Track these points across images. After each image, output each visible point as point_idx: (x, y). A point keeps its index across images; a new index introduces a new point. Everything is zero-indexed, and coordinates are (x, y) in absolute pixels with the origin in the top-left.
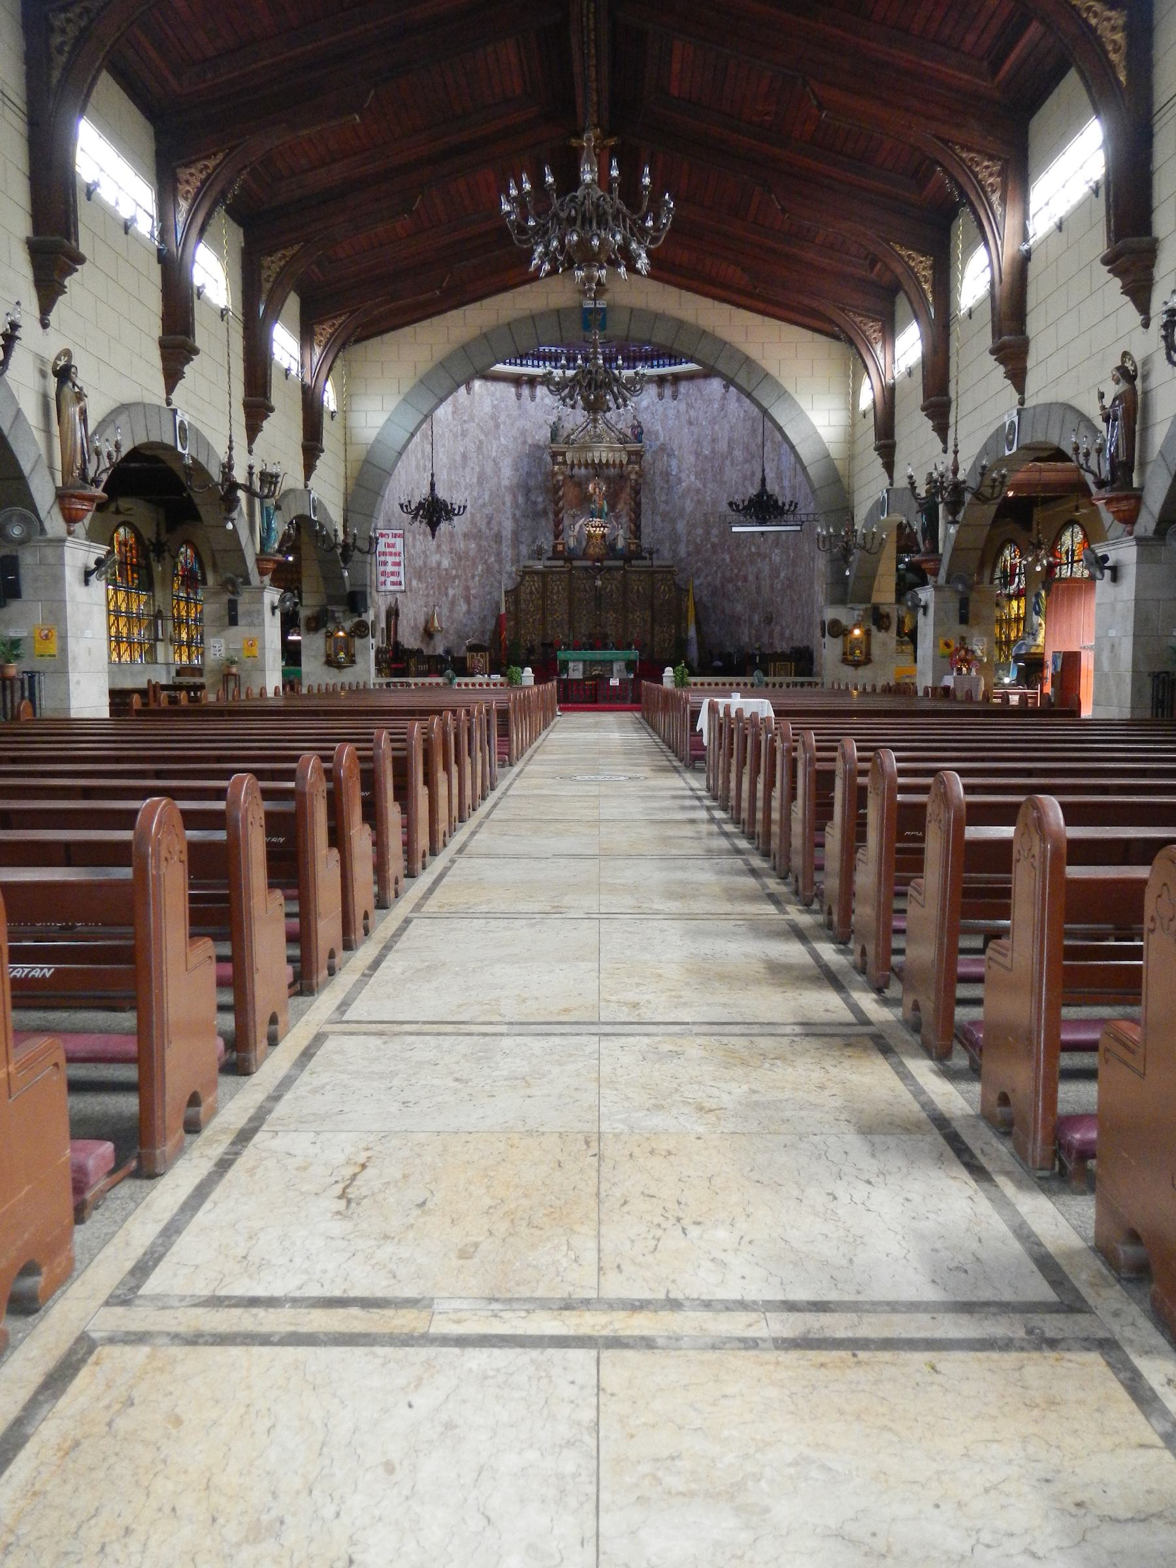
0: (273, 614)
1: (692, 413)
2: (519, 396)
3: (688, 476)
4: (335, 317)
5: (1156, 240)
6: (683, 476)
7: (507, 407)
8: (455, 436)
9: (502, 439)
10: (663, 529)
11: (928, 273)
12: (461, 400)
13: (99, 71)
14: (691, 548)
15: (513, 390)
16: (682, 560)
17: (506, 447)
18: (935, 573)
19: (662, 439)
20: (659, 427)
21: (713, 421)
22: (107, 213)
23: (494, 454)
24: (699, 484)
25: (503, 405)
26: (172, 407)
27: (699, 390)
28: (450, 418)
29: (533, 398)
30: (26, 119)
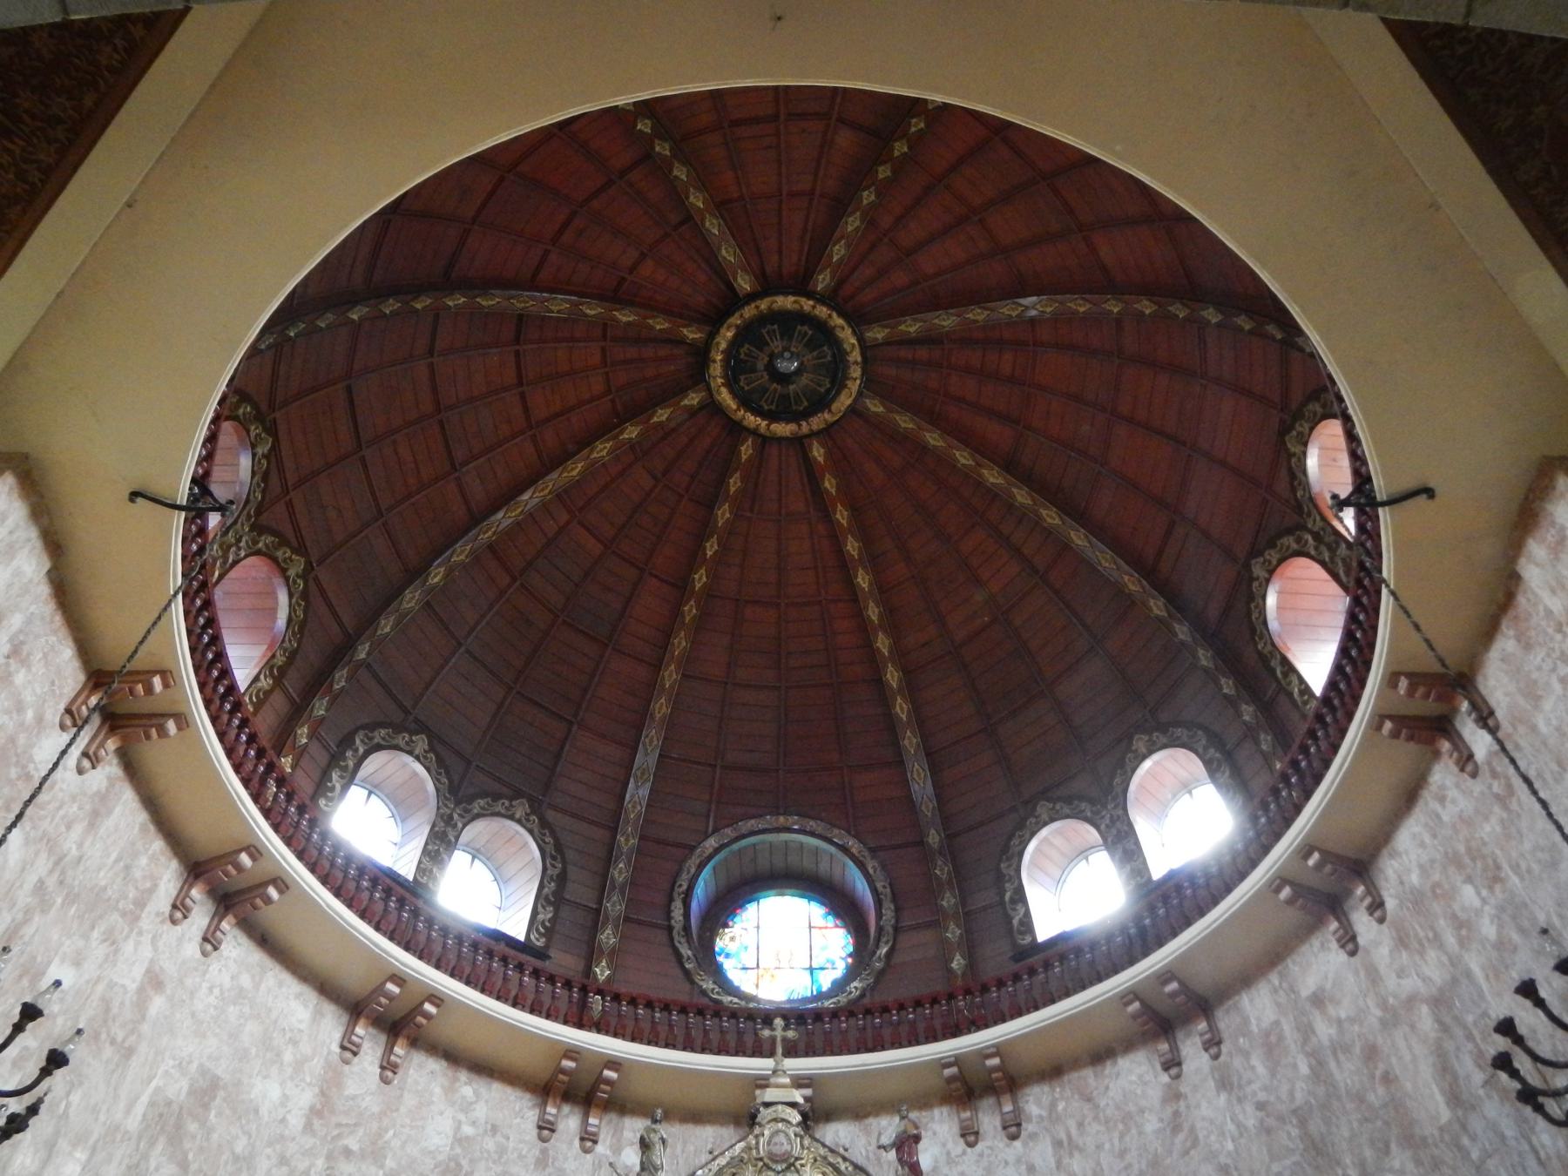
2: (546, 1128)
7: (502, 1151)
12: (351, 1088)
15: (532, 1116)
25: (490, 1144)
27: (1089, 1100)
28: (296, 1121)
29: (588, 1139)
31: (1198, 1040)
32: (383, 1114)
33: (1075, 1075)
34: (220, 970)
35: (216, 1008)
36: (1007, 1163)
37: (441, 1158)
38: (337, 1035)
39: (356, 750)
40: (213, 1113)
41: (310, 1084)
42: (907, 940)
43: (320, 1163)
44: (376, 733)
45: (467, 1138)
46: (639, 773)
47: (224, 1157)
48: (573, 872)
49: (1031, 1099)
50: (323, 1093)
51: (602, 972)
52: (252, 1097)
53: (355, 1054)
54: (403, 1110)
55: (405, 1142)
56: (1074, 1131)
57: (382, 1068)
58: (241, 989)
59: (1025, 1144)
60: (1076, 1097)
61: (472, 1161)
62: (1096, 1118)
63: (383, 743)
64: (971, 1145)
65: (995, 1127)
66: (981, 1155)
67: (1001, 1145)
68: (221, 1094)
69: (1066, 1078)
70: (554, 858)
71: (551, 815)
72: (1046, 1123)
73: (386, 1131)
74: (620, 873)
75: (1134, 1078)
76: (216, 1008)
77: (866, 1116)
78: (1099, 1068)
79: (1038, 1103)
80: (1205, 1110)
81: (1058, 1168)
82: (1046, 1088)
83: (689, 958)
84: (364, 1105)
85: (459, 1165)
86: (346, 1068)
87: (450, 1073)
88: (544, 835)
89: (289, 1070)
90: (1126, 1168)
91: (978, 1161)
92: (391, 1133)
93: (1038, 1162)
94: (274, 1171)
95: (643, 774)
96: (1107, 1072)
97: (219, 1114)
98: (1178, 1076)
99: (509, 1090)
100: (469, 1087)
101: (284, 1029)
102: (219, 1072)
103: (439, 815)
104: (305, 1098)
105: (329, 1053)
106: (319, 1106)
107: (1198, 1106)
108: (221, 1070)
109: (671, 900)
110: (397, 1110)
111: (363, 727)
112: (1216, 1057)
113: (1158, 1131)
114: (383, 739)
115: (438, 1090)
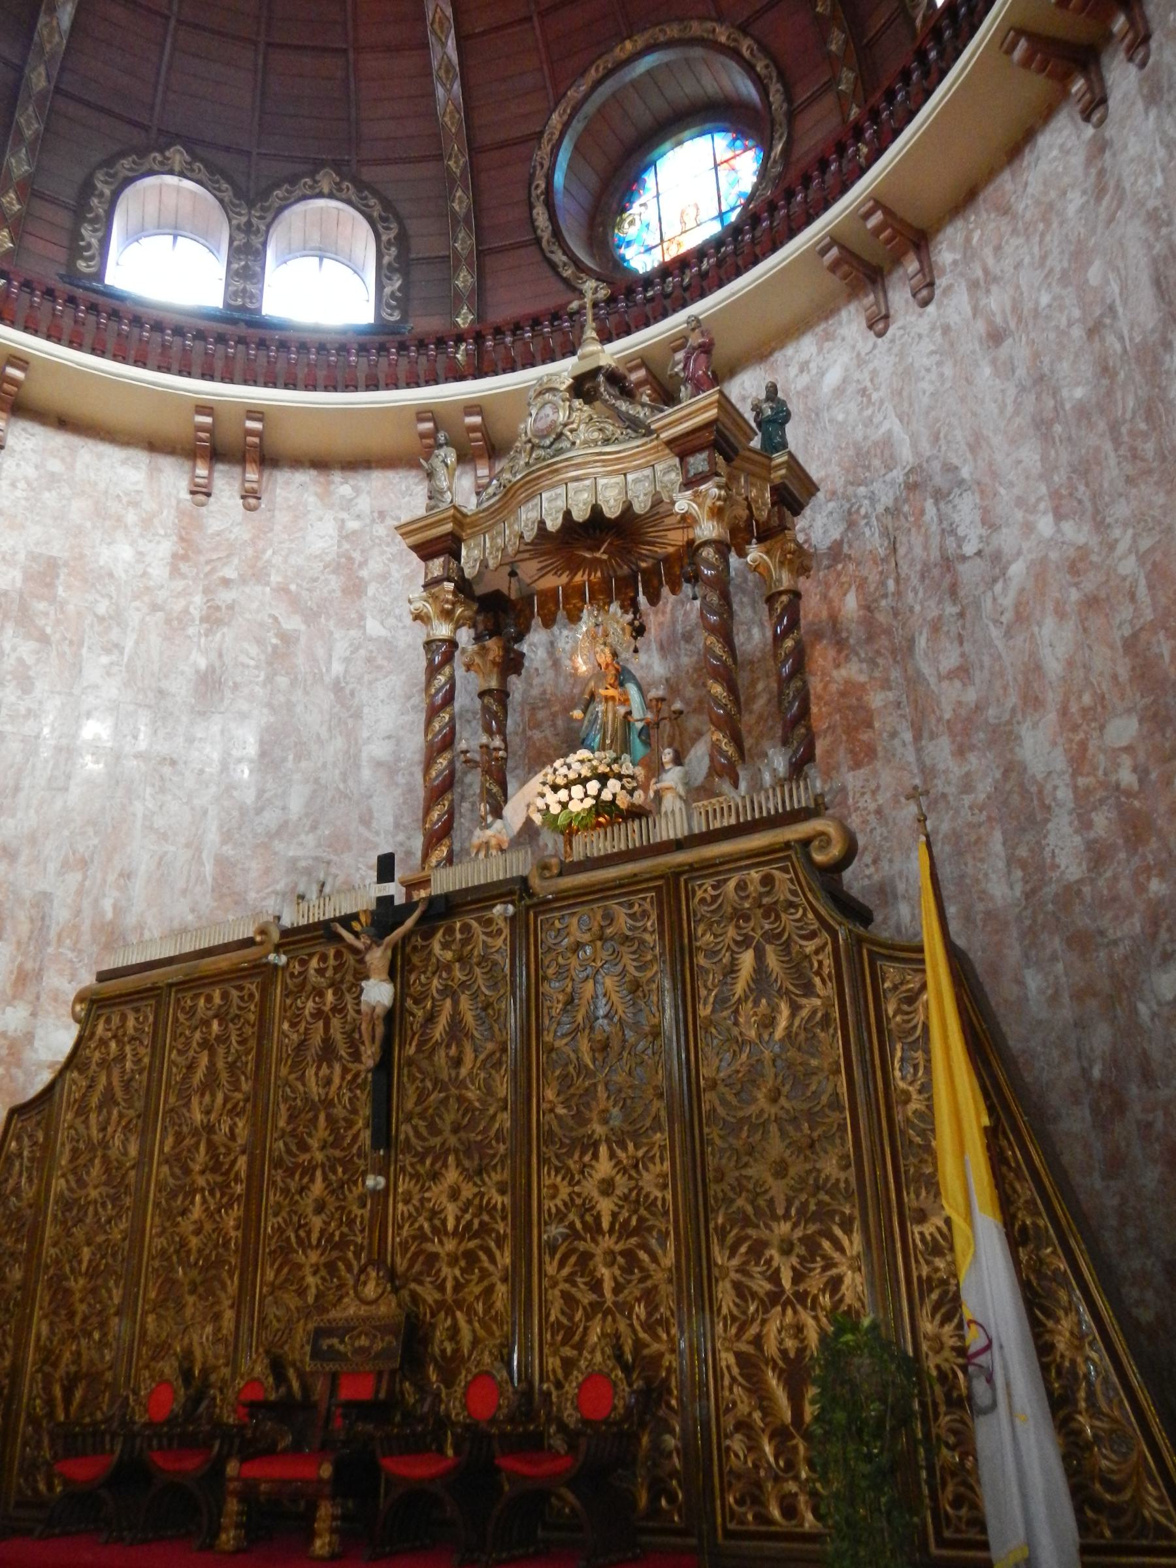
1: (996, 301)
3: (1028, 528)
6: (1008, 539)
8: (175, 624)
9: (373, 627)
10: (967, 786)
14: (1102, 821)
16: (1071, 892)
17: (388, 646)
19: (906, 454)
20: (891, 424)
21: (1080, 255)
23: (337, 668)
24: (1076, 533)
28: (159, 571)
31: (1121, 55)
32: (253, 541)
33: (991, 188)
34: (18, 465)
35: (27, 499)
36: (920, 336)
37: (328, 559)
38: (183, 485)
39: (102, 195)
40: (60, 591)
41: (166, 535)
42: (806, 121)
43: (198, 599)
44: (118, 166)
45: (354, 533)
46: (442, 73)
47: (88, 622)
48: (413, 226)
49: (944, 246)
50: (182, 539)
51: (464, 319)
52: (102, 563)
53: (208, 495)
54: (278, 528)
55: (287, 556)
56: (990, 261)
57: (243, 497)
58: (53, 474)
59: (939, 307)
60: (993, 216)
61: (363, 551)
62: (1015, 232)
63: (130, 174)
64: (880, 335)
65: (907, 301)
66: (892, 341)
67: (913, 319)
68: (63, 572)
69: (981, 198)
70: (384, 220)
71: (368, 174)
72: (960, 268)
73: (264, 551)
74: (461, 202)
75: (1055, 153)
76: (27, 499)
77: (771, 353)
78: (1016, 163)
79: (952, 248)
80: (1134, 148)
81: (974, 315)
82: (959, 223)
83: (565, 264)
84: (233, 536)
85: (350, 559)
86: (203, 510)
87: (322, 479)
88: (366, 198)
89: (137, 530)
90: (1047, 276)
91: (890, 349)
92: (269, 552)
93: (954, 319)
94: (148, 618)
95: (447, 72)
96: (1025, 163)
97: (68, 587)
98: (1102, 121)
99: (391, 475)
100: (343, 486)
101: (118, 496)
102: (54, 553)
103: (235, 229)
104: (166, 548)
105: (179, 502)
106: (181, 552)
107: (1125, 147)
108: (58, 549)
109: (531, 207)
110: (272, 530)
111: (100, 166)
112: (1143, 65)
113: (1082, 208)
114: (131, 170)
115: (312, 499)
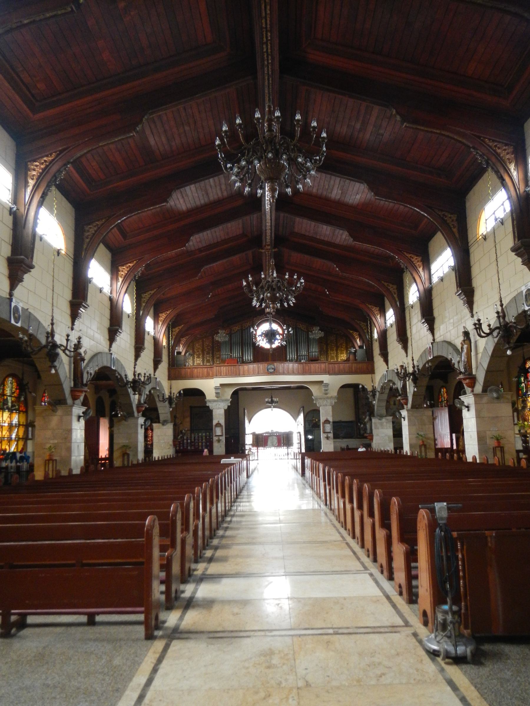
0: (142, 428)
4: (167, 311)
5: (474, 287)
11: (395, 291)
13: (99, 244)
18: (407, 404)
22: (95, 286)
26: (111, 352)
30: (73, 260)
